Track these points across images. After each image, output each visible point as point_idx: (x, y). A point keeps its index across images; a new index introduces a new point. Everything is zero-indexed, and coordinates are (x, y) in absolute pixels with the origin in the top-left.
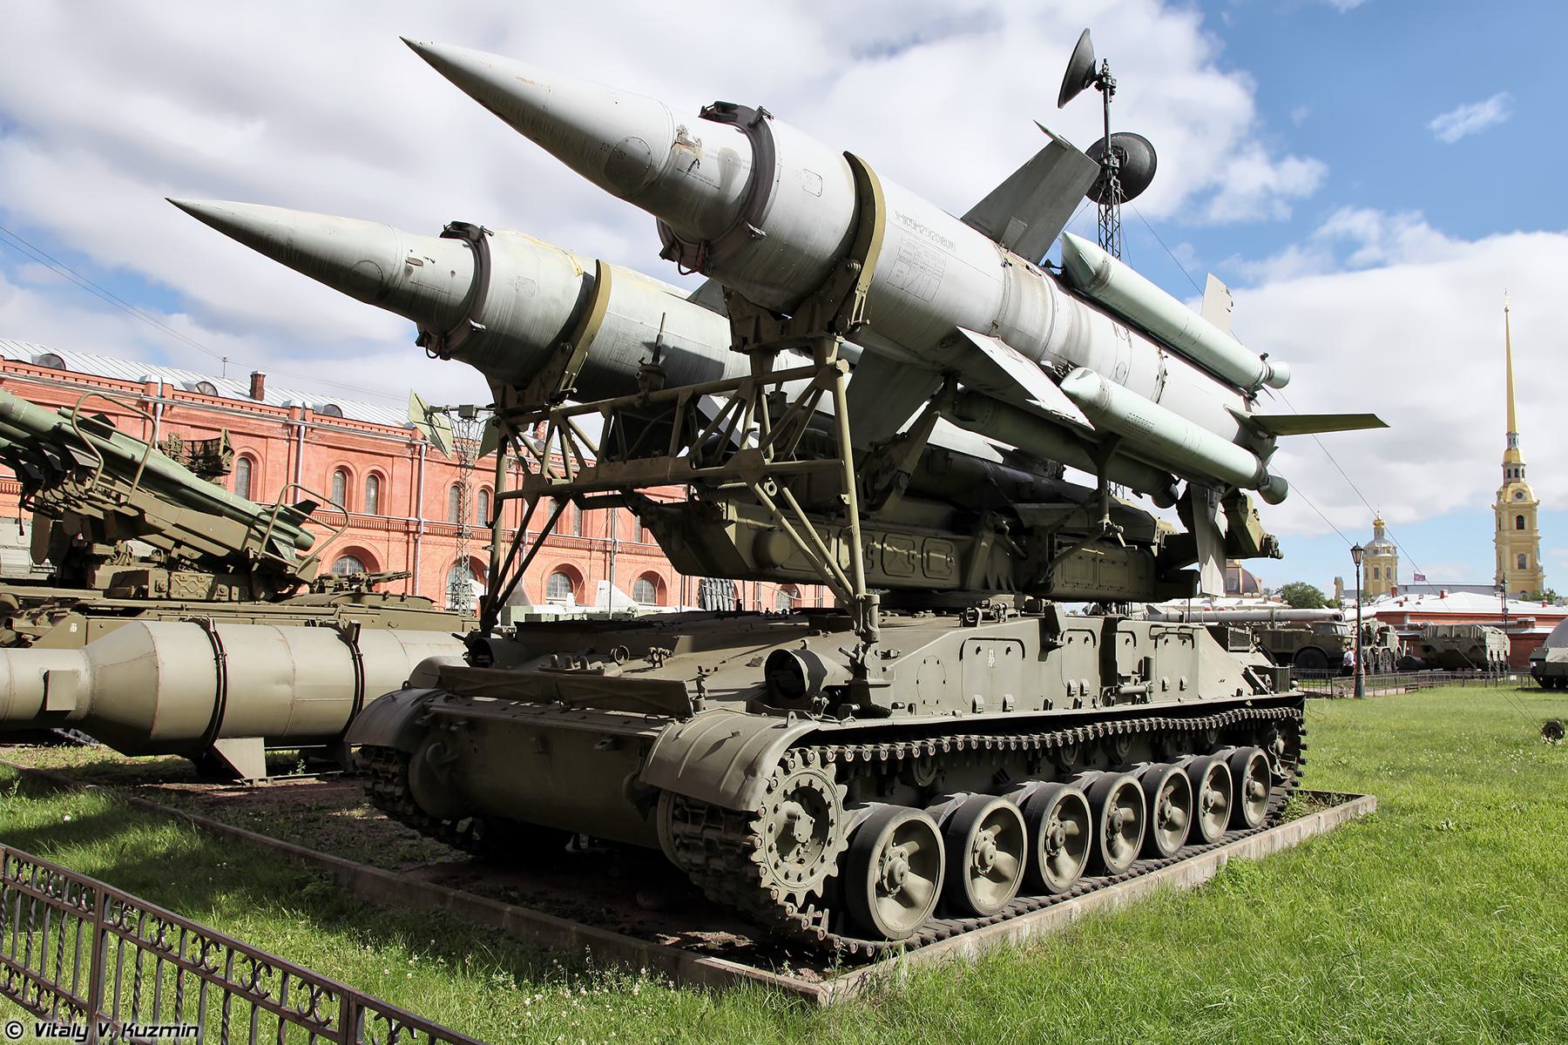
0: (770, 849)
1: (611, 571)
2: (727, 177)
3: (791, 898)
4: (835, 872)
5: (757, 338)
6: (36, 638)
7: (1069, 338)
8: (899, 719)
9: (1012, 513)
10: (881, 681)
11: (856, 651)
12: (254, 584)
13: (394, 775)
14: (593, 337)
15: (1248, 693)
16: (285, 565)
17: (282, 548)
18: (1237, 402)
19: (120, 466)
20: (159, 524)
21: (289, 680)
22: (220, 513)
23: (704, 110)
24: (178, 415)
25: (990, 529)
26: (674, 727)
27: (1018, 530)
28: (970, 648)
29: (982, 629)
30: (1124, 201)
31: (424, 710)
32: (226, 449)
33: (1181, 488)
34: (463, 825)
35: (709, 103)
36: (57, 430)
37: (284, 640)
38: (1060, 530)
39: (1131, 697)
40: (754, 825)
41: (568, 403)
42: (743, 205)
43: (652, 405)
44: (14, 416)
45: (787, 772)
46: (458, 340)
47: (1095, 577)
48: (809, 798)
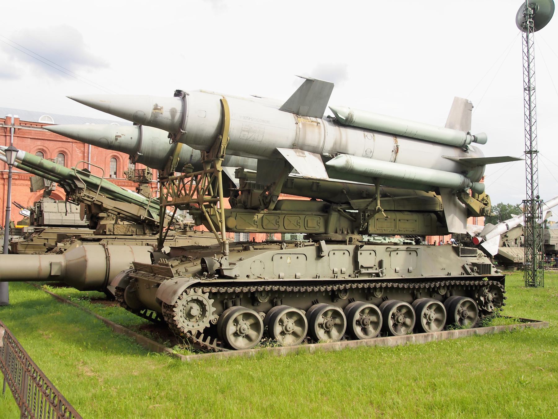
3: (190, 332)
6: (65, 250)
7: (335, 144)
10: (229, 267)
12: (145, 228)
18: (455, 154)
19: (92, 186)
22: (130, 202)
25: (335, 211)
28: (277, 258)
30: (535, 31)
32: (148, 173)
34: (149, 312)
37: (132, 251)
40: (174, 309)
44: (56, 171)
46: (136, 158)
47: (395, 227)
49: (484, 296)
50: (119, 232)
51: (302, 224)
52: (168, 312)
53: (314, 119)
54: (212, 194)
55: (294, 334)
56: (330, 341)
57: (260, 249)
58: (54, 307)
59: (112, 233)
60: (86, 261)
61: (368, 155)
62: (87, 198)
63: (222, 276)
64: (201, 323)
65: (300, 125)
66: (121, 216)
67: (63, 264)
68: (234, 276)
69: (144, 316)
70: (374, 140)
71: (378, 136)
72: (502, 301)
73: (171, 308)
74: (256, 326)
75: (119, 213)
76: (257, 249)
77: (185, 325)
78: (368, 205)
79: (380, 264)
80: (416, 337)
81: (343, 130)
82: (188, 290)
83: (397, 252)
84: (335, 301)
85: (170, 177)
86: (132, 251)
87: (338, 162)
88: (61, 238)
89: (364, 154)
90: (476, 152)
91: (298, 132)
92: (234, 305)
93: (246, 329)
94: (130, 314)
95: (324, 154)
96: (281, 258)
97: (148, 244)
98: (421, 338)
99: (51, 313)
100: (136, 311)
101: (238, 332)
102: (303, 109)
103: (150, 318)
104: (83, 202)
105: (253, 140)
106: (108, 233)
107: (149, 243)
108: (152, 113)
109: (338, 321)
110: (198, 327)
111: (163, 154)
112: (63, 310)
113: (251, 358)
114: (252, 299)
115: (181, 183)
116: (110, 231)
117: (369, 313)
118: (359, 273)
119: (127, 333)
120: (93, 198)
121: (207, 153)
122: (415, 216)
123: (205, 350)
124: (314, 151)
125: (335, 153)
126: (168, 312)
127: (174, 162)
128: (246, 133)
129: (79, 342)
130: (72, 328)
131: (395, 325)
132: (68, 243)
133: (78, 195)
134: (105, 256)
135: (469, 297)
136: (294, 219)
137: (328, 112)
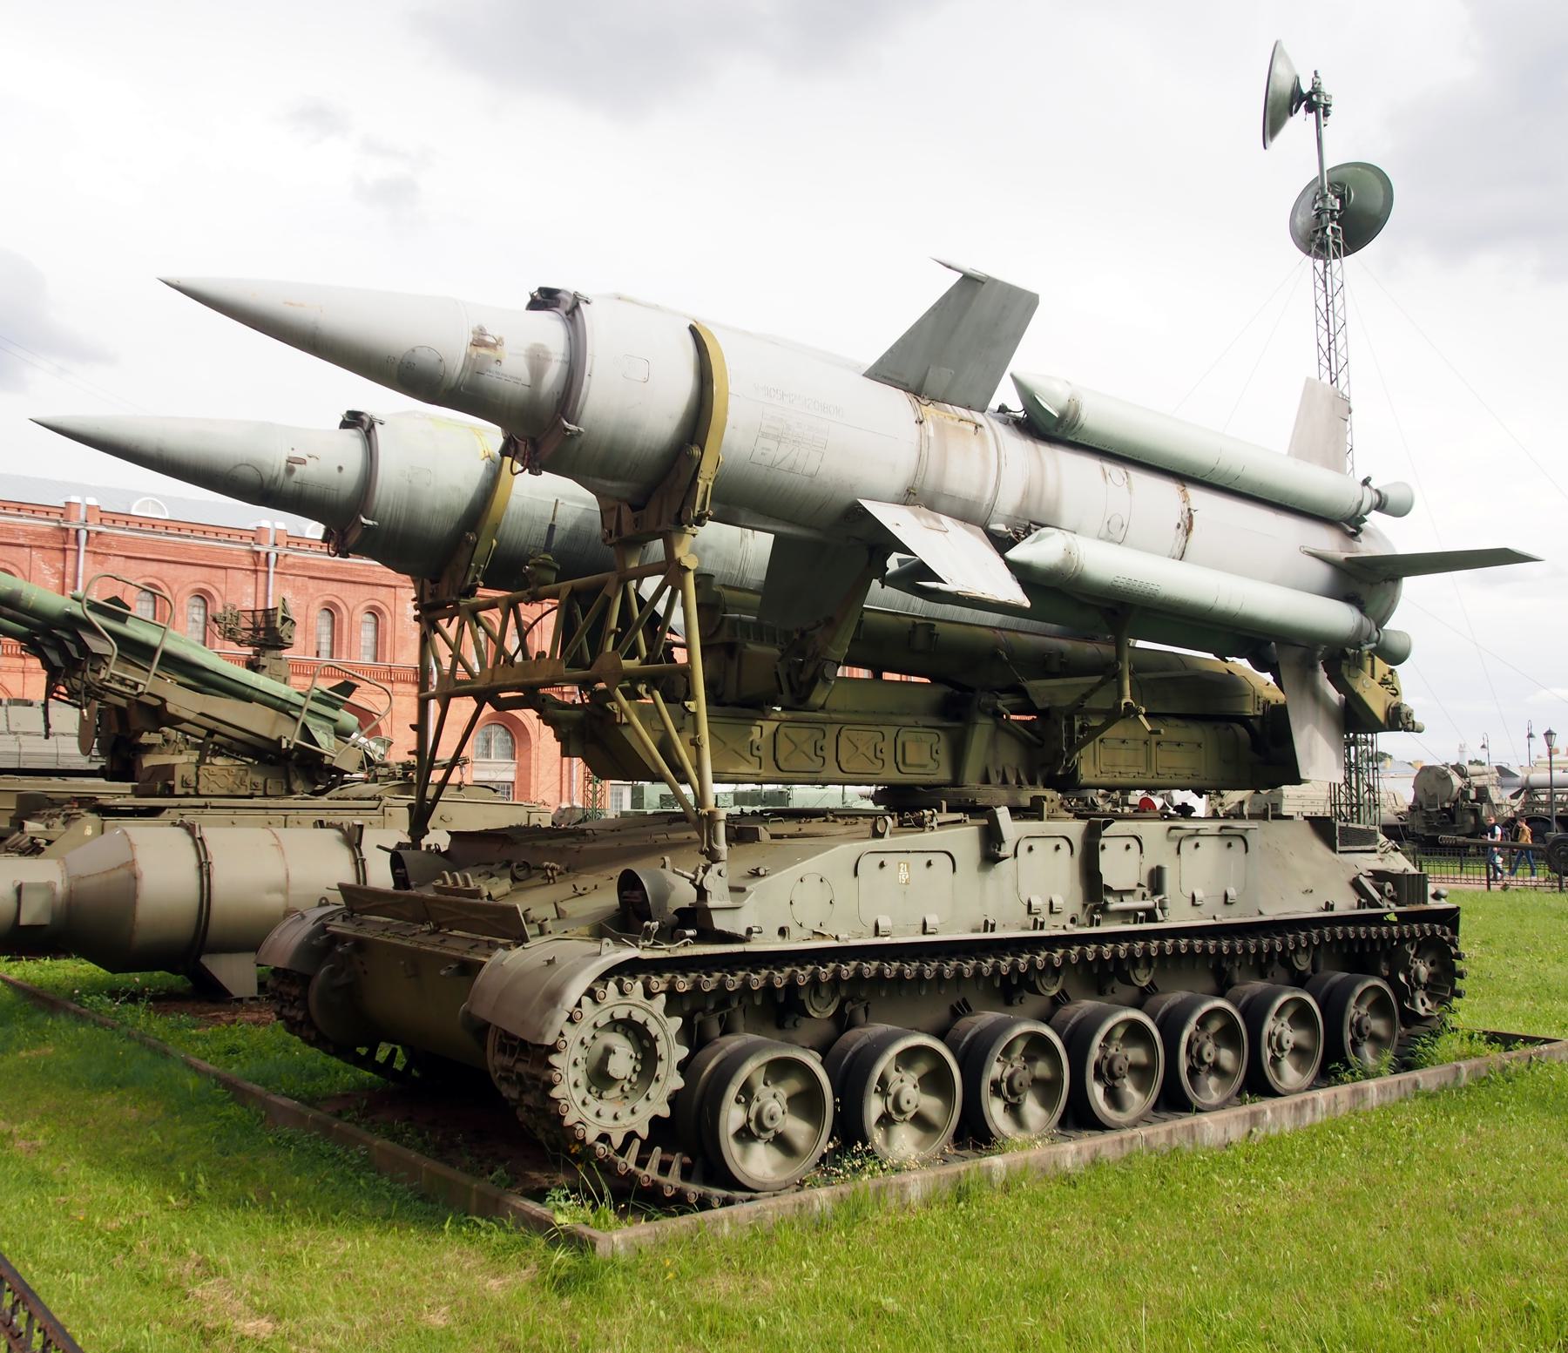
0: (576, 1085)
2: (537, 371)
3: (604, 1138)
4: (665, 1112)
6: (49, 842)
7: (1027, 494)
9: (1019, 691)
10: (728, 903)
11: (696, 873)
12: (292, 778)
13: (296, 999)
14: (497, 526)
16: (323, 755)
17: (319, 736)
21: (284, 889)
22: (249, 699)
24: (293, 566)
25: (985, 714)
26: (517, 952)
29: (887, 842)
31: (322, 929)
32: (285, 619)
34: (382, 1055)
36: (71, 618)
37: (279, 846)
38: (1077, 709)
40: (554, 1059)
42: (559, 401)
44: (23, 603)
45: (596, 1002)
46: (354, 537)
49: (1407, 971)
50: (213, 786)
51: (888, 755)
52: (521, 1068)
53: (964, 413)
54: (644, 653)
55: (920, 1121)
56: (1028, 1139)
57: (790, 837)
58: (29, 1027)
59: (192, 791)
60: (135, 877)
61: (1114, 534)
62: (117, 686)
63: (709, 934)
64: (641, 1104)
65: (929, 426)
66: (217, 741)
67: (60, 888)
68: (743, 933)
69: (368, 1062)
70: (1130, 489)
71: (1140, 479)
72: (1453, 984)
73: (542, 1054)
74: (806, 1103)
75: (211, 733)
76: (780, 837)
77: (589, 1113)
78: (1085, 696)
79: (1156, 880)
80: (1273, 1111)
81: (1046, 451)
82: (599, 990)
83: (1197, 840)
84: (1016, 1001)
85: (463, 602)
86: (279, 846)
87: (1037, 551)
88: (30, 806)
89: (1104, 532)
90: (1388, 536)
91: (924, 451)
92: (727, 1030)
93: (780, 1115)
94: (316, 1058)
95: (993, 527)
96: (882, 865)
97: (321, 824)
98: (1285, 1112)
99: (20, 1048)
100: (342, 1050)
101: (752, 1125)
102: (939, 378)
103: (385, 1069)
104: (97, 696)
105: (791, 470)
106: (178, 790)
107: (327, 819)
108: (468, 356)
109: (1042, 1069)
110: (633, 1119)
111: (443, 526)
112: (57, 1044)
113: (820, 1225)
114: (780, 1010)
115: (481, 630)
116: (185, 784)
117: (1123, 1039)
118: (1104, 909)
119: (327, 1130)
120: (135, 686)
121: (634, 508)
122: (1195, 733)
123: (679, 1204)
124: (969, 515)
125: (1027, 526)
126: (521, 1068)
127: (481, 551)
128: (772, 445)
129: (157, 1166)
130: (105, 1102)
131: (1193, 1072)
132: (58, 822)
133: (90, 675)
134: (193, 861)
135: (1365, 980)
136: (865, 738)
137: (1006, 396)
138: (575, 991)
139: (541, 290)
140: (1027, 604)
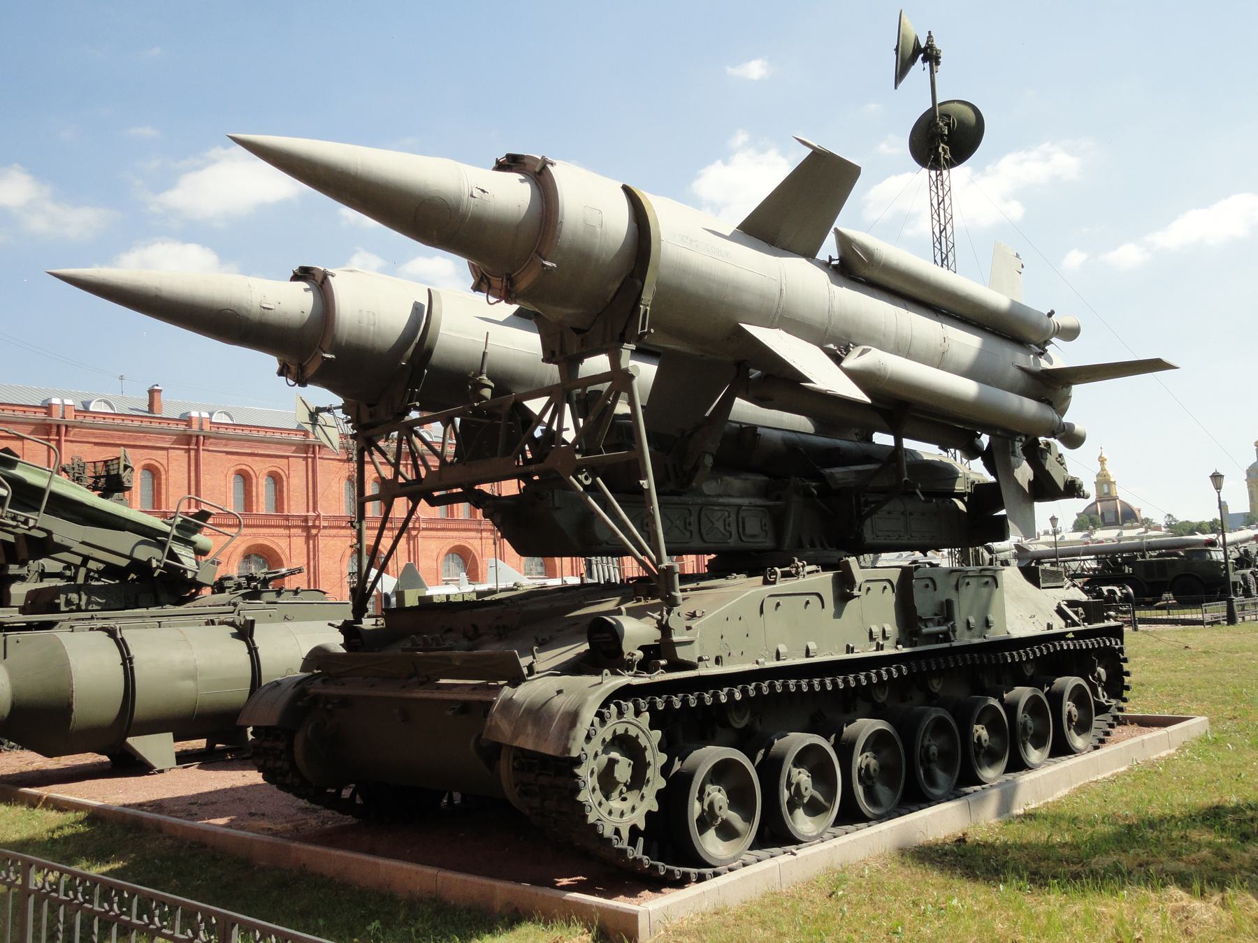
0: (594, 790)
1: (460, 560)
4: (655, 808)
5: (562, 352)
8: (703, 671)
9: (820, 478)
15: (1059, 626)
16: (185, 570)
20: (67, 543)
23: (497, 162)
27: (828, 491)
28: (769, 604)
29: (782, 585)
32: (126, 467)
33: (985, 440)
34: (346, 793)
35: (501, 156)
39: (934, 638)
41: (414, 415)
43: (485, 409)
46: (311, 370)
48: (626, 744)
61: (904, 349)
75: (86, 559)
106: (63, 608)
118: (917, 633)
138: (588, 716)
139: (508, 156)
140: (868, 400)
